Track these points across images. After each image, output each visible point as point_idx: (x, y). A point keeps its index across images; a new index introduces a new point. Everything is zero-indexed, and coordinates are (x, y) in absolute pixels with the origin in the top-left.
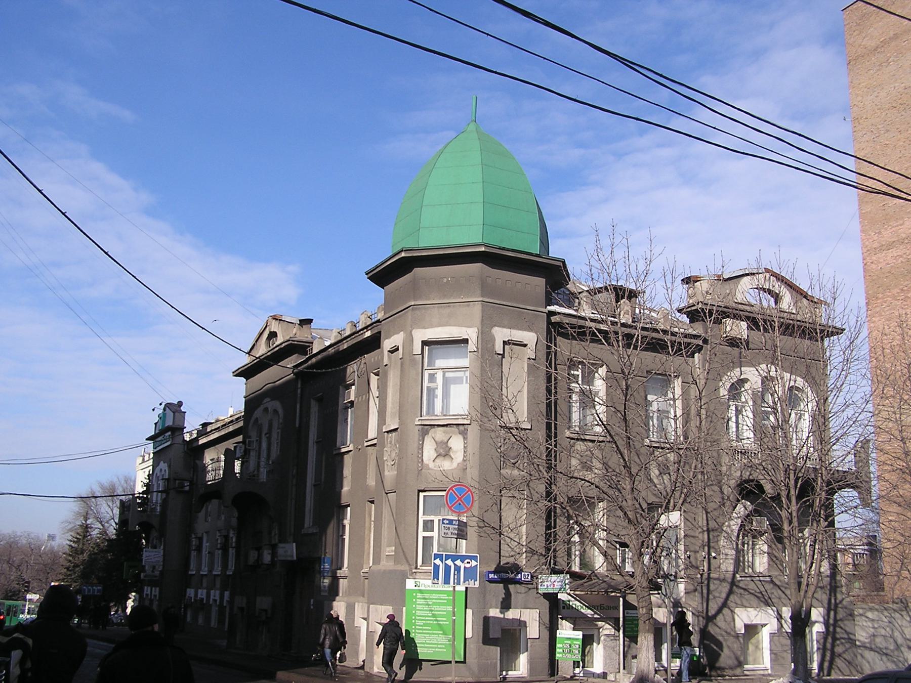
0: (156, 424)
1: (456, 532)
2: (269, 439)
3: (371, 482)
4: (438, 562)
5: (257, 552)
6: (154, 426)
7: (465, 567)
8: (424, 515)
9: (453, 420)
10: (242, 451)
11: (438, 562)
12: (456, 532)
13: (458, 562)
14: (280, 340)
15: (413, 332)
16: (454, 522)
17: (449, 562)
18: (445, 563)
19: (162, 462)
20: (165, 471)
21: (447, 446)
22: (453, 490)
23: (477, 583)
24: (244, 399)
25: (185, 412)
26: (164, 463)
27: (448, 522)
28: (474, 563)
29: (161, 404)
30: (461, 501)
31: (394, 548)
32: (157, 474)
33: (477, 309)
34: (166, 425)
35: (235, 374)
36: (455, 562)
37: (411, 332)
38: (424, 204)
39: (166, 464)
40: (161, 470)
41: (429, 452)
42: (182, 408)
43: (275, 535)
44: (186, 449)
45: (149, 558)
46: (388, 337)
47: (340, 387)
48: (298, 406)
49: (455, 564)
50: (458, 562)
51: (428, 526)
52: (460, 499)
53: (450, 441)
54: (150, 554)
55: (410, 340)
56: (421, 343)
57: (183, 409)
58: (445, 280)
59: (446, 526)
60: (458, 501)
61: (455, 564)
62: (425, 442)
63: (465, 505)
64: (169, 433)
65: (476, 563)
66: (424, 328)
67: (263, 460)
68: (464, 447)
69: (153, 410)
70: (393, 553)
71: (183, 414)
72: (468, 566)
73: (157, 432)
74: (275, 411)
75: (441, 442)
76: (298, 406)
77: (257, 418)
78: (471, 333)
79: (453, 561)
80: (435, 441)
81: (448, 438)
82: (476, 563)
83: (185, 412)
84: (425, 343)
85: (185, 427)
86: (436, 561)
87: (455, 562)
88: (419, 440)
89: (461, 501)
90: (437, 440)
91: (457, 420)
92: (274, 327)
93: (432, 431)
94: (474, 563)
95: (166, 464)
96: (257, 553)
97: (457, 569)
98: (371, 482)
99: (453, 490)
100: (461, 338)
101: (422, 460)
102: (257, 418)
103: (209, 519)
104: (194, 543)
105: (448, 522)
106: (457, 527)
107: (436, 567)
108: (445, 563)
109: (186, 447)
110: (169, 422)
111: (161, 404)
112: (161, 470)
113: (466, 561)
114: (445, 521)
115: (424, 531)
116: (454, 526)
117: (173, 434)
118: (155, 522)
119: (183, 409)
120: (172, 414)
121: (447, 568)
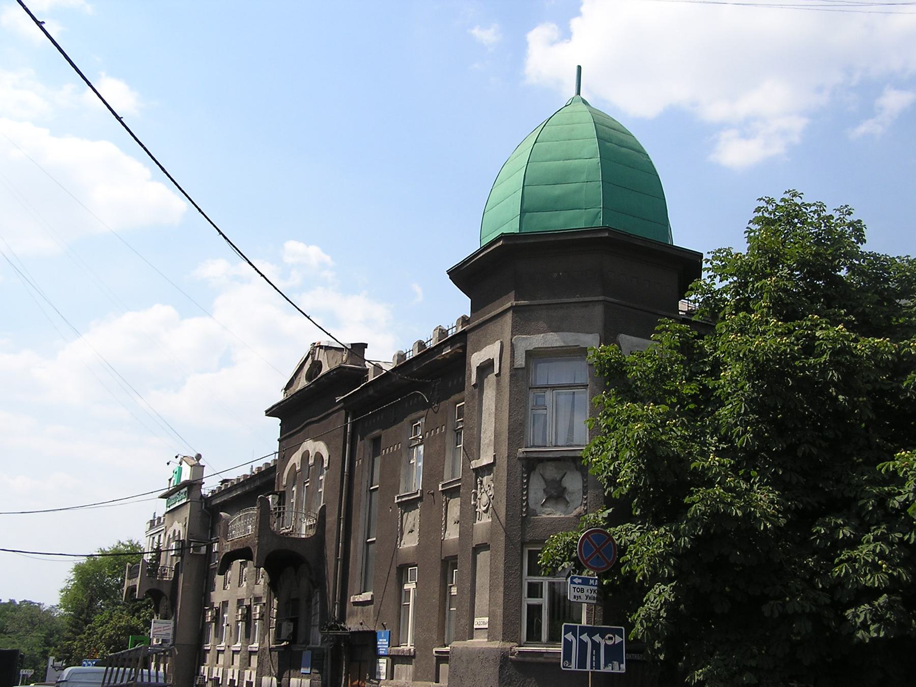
1: (595, 595)
3: (452, 534)
4: (570, 636)
5: (292, 624)
7: (606, 645)
8: (529, 575)
9: (568, 452)
10: (275, 503)
11: (570, 636)
12: (595, 595)
13: (597, 638)
14: (325, 369)
16: (591, 582)
17: (585, 637)
18: (579, 638)
19: (176, 523)
20: (179, 532)
21: (561, 486)
22: (589, 538)
23: (623, 666)
24: (278, 442)
25: (204, 466)
26: (178, 523)
27: (580, 581)
28: (618, 639)
29: (177, 457)
30: (600, 553)
31: (487, 619)
32: (169, 536)
33: (599, 310)
34: (182, 480)
35: (269, 413)
38: (525, 185)
39: (181, 524)
40: (175, 531)
41: (535, 493)
43: (316, 604)
44: (203, 508)
45: (160, 629)
46: (478, 348)
49: (593, 641)
50: (597, 638)
51: (535, 590)
52: (598, 550)
53: (563, 479)
57: (201, 462)
58: (555, 275)
60: (595, 553)
61: (593, 641)
62: (531, 482)
63: (604, 558)
64: (186, 489)
65: (622, 640)
68: (583, 487)
69: (168, 464)
70: (487, 626)
71: (202, 468)
72: (610, 643)
75: (554, 481)
77: (295, 464)
79: (590, 636)
80: (544, 478)
81: (560, 476)
82: (622, 640)
83: (204, 466)
84: (529, 354)
85: (204, 483)
88: (523, 478)
89: (600, 553)
90: (546, 478)
91: (574, 452)
92: (321, 356)
93: (539, 468)
94: (618, 639)
95: (181, 524)
96: (292, 624)
97: (596, 646)
98: (452, 534)
99: (589, 538)
100: (578, 347)
101: (527, 504)
102: (295, 464)
103: (228, 586)
105: (580, 581)
106: (596, 588)
107: (568, 645)
110: (186, 476)
111: (177, 457)
112: (175, 531)
113: (607, 637)
114: (576, 580)
115: (528, 597)
116: (592, 588)
118: (166, 590)
119: (201, 462)
120: (190, 467)
121: (583, 645)
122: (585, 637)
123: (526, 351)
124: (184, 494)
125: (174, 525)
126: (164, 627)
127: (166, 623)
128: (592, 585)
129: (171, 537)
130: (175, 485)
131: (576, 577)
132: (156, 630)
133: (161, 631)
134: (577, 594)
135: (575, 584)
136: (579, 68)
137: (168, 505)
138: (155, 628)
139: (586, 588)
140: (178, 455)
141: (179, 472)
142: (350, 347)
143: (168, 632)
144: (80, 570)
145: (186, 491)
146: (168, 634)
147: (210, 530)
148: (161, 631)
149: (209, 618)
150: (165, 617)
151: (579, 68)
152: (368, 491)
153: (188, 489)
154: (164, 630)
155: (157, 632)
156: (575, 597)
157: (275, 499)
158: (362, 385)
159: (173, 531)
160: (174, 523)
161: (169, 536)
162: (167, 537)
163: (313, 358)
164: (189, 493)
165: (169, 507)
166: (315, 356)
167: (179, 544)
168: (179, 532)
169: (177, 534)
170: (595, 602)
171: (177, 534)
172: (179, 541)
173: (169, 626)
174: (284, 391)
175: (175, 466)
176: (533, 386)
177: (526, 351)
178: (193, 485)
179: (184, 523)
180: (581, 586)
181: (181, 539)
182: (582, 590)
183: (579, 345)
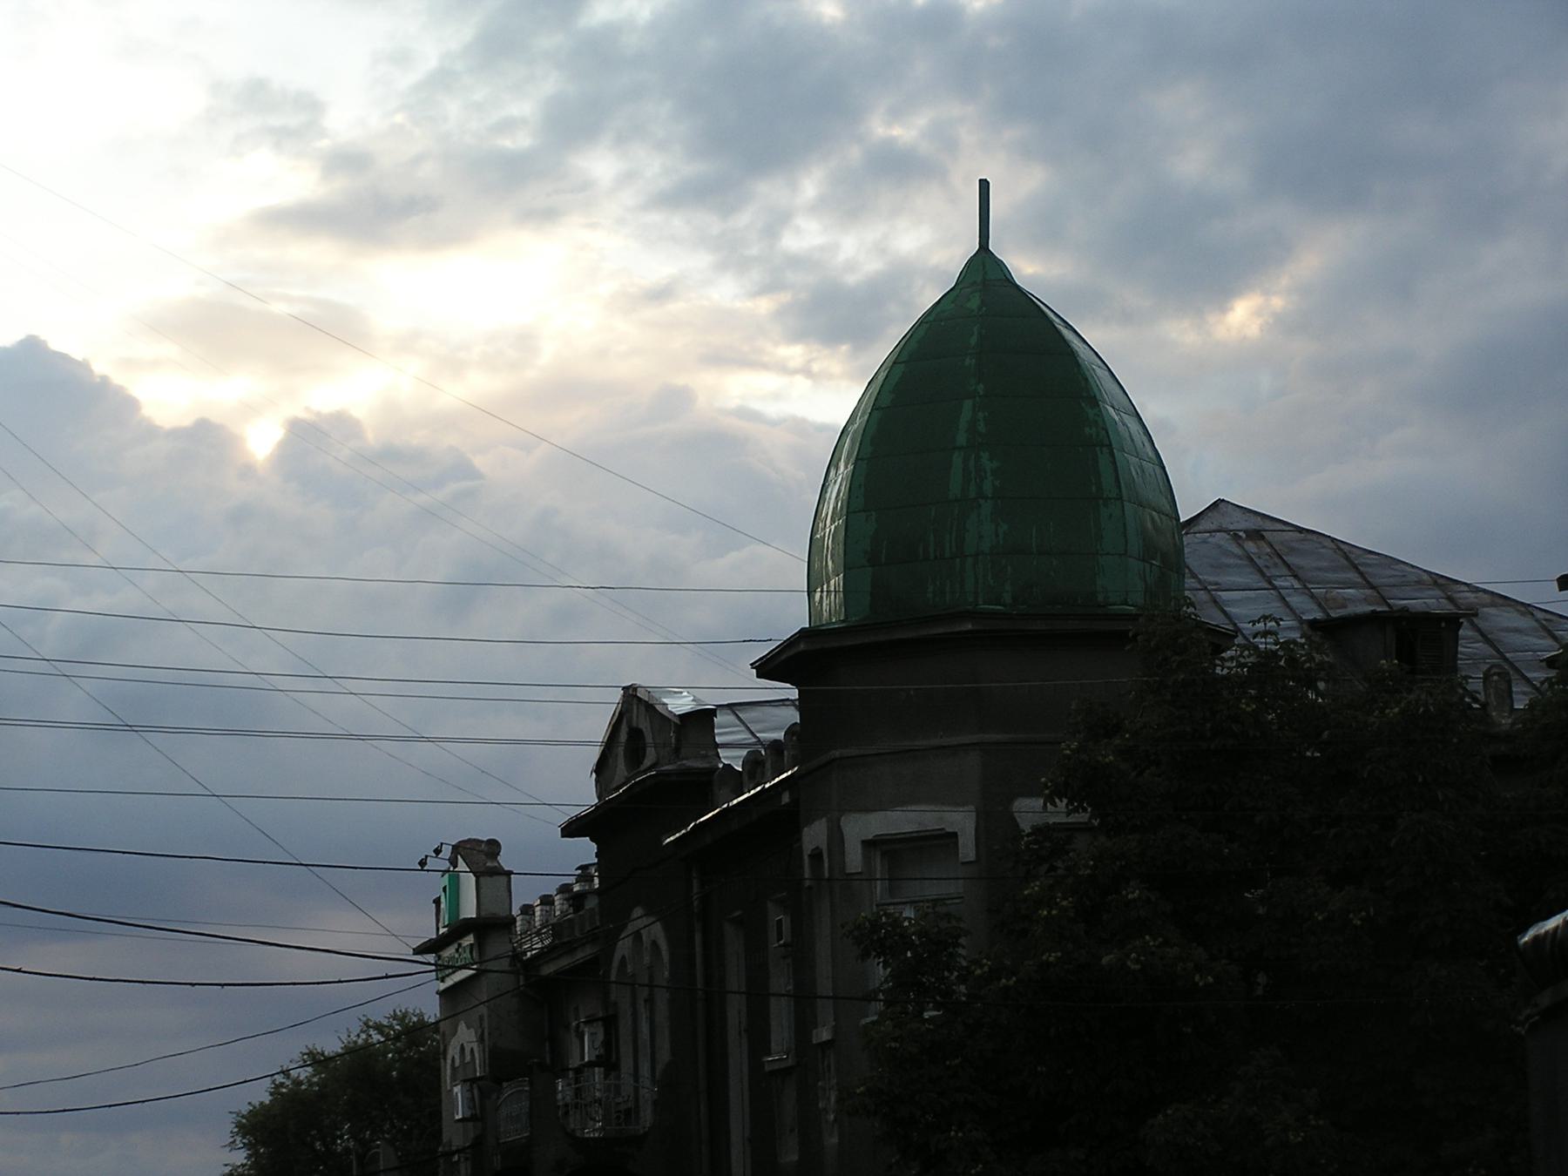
0: (437, 902)
2: (652, 1012)
10: (597, 1044)
19: (462, 1027)
20: (472, 1050)
26: (468, 1028)
29: (438, 851)
34: (462, 917)
37: (839, 820)
39: (472, 1031)
47: (770, 905)
48: (698, 938)
55: (836, 836)
56: (859, 846)
57: (505, 861)
64: (469, 940)
66: (867, 810)
67: (645, 1069)
71: (503, 879)
73: (442, 931)
74: (654, 944)
76: (698, 938)
77: (623, 957)
78: (961, 821)
95: (472, 1031)
100: (943, 832)
109: (521, 977)
117: (480, 944)
124: (468, 951)
125: (459, 1032)
129: (457, 1064)
130: (446, 923)
136: (984, 185)
137: (440, 976)
140: (442, 844)
141: (454, 889)
142: (677, 721)
145: (471, 944)
147: (547, 1044)
151: (984, 185)
152: (743, 1032)
157: (596, 1034)
158: (672, 838)
159: (458, 1048)
160: (459, 1029)
162: (449, 1061)
165: (443, 980)
166: (631, 717)
167: (471, 1090)
168: (472, 1050)
169: (468, 1058)
171: (468, 1058)
172: (473, 1080)
174: (594, 775)
176: (883, 901)
178: (490, 927)
179: (480, 1031)
181: (478, 1074)
183: (943, 829)
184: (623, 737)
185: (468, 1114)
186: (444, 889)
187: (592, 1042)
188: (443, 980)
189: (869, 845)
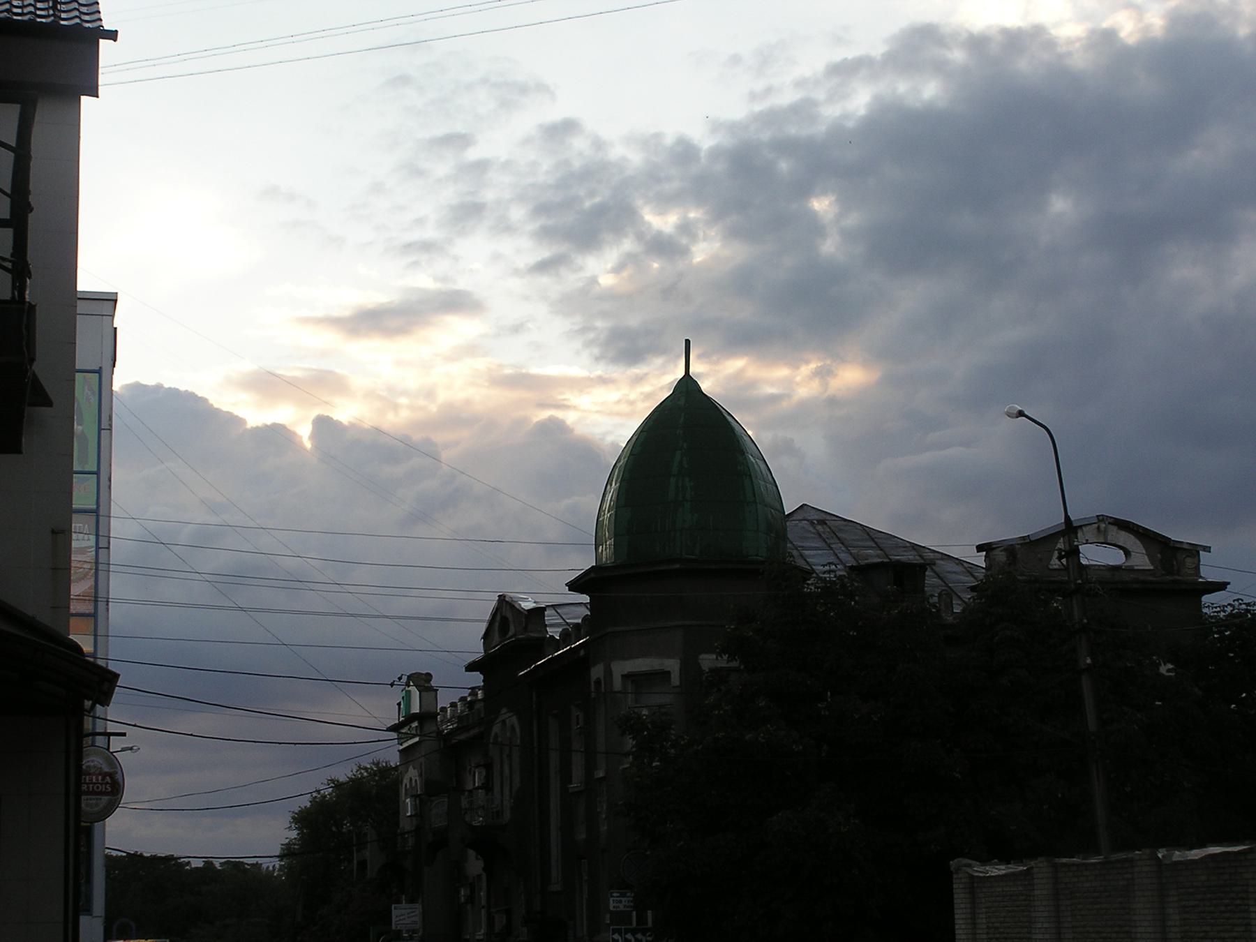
0: (399, 704)
6: (397, 707)
10: (482, 777)
12: (632, 904)
15: (612, 666)
17: (629, 936)
18: (625, 938)
20: (416, 780)
26: (414, 769)
29: (400, 679)
32: (406, 785)
34: (412, 712)
36: (637, 936)
37: (610, 665)
40: (411, 779)
42: (431, 682)
44: (442, 746)
45: (404, 917)
54: (403, 911)
55: (609, 673)
56: (620, 678)
57: (433, 683)
59: (615, 899)
61: (635, 938)
64: (415, 724)
67: (507, 792)
71: (433, 693)
73: (401, 719)
74: (513, 728)
77: (496, 734)
78: (672, 665)
79: (633, 935)
86: (627, 936)
87: (637, 936)
95: (416, 771)
104: (463, 894)
108: (625, 938)
112: (411, 779)
113: (648, 934)
116: (629, 899)
117: (421, 726)
119: (433, 683)
122: (629, 936)
123: (622, 676)
126: (408, 914)
127: (411, 908)
128: (629, 897)
129: (408, 787)
131: (613, 892)
132: (398, 919)
133: (404, 919)
134: (615, 904)
135: (614, 897)
138: (397, 916)
139: (623, 899)
140: (402, 675)
143: (413, 919)
144: (303, 819)
145: (416, 726)
146: (415, 923)
148: (404, 919)
149: (463, 898)
150: (412, 901)
153: (419, 723)
154: (408, 917)
155: (400, 920)
156: (614, 907)
158: (523, 673)
160: (410, 770)
161: (406, 785)
163: (501, 614)
164: (421, 731)
165: (401, 745)
167: (415, 801)
169: (414, 785)
170: (631, 909)
171: (414, 785)
173: (414, 912)
175: (397, 694)
177: (622, 676)
178: (426, 717)
179: (420, 771)
180: (618, 899)
181: (419, 793)
182: (620, 902)
184: (498, 618)
185: (413, 813)
186: (403, 698)
187: (479, 778)
188: (401, 745)
189: (625, 677)
